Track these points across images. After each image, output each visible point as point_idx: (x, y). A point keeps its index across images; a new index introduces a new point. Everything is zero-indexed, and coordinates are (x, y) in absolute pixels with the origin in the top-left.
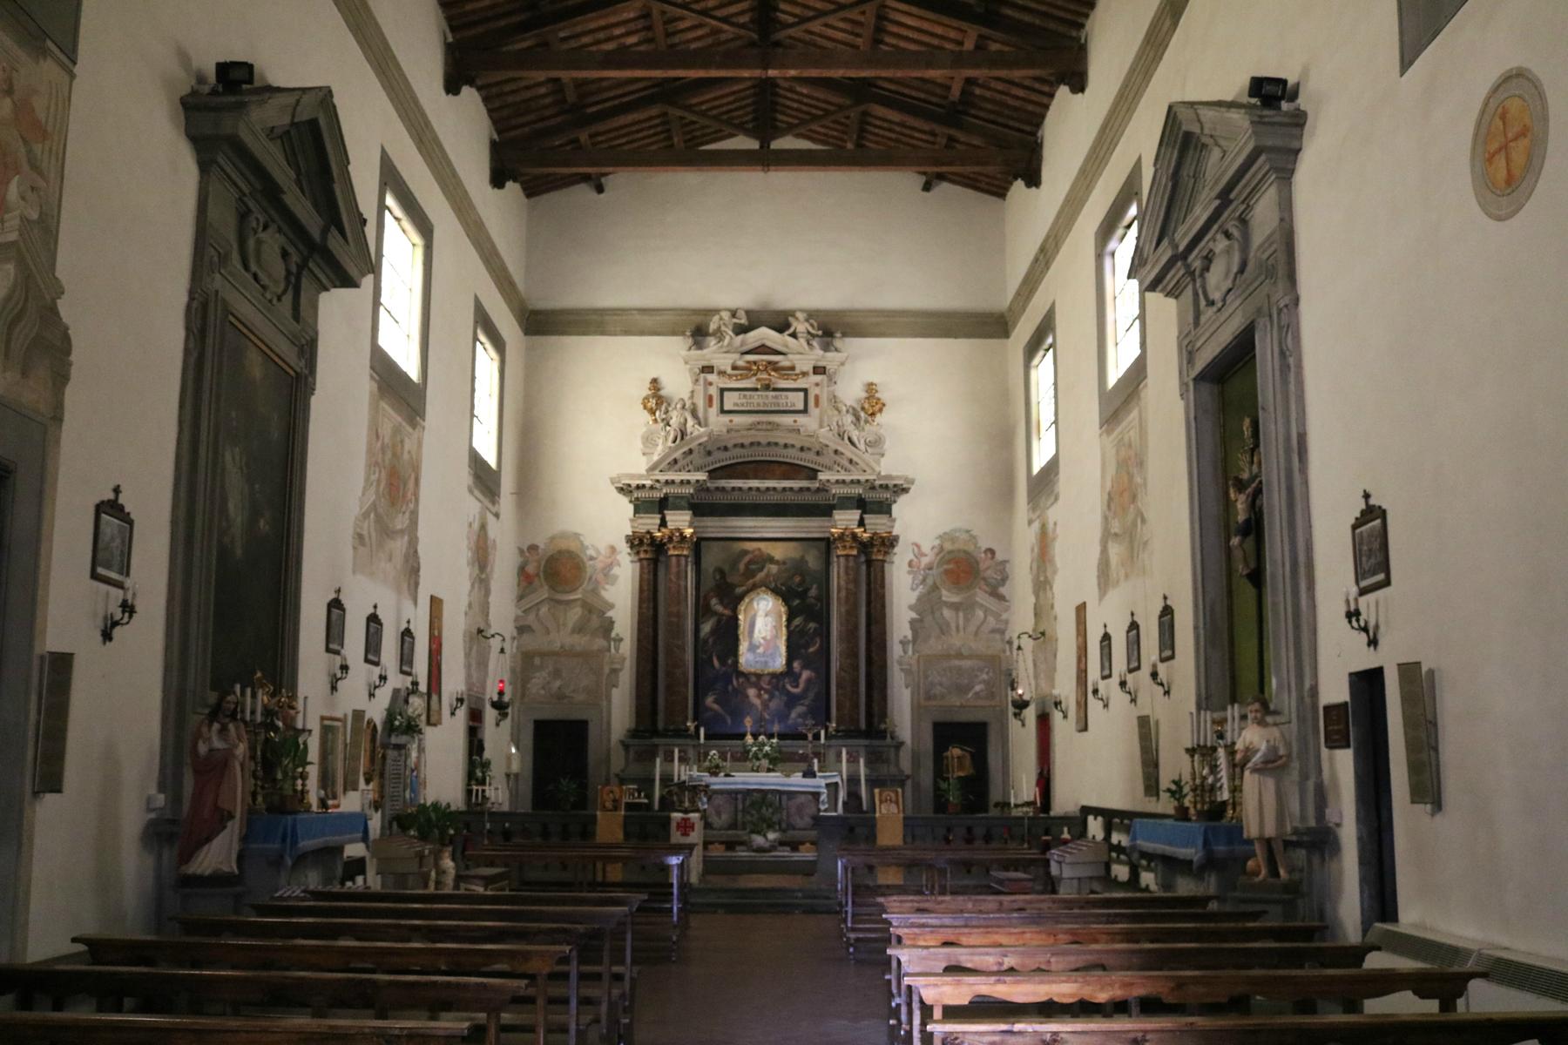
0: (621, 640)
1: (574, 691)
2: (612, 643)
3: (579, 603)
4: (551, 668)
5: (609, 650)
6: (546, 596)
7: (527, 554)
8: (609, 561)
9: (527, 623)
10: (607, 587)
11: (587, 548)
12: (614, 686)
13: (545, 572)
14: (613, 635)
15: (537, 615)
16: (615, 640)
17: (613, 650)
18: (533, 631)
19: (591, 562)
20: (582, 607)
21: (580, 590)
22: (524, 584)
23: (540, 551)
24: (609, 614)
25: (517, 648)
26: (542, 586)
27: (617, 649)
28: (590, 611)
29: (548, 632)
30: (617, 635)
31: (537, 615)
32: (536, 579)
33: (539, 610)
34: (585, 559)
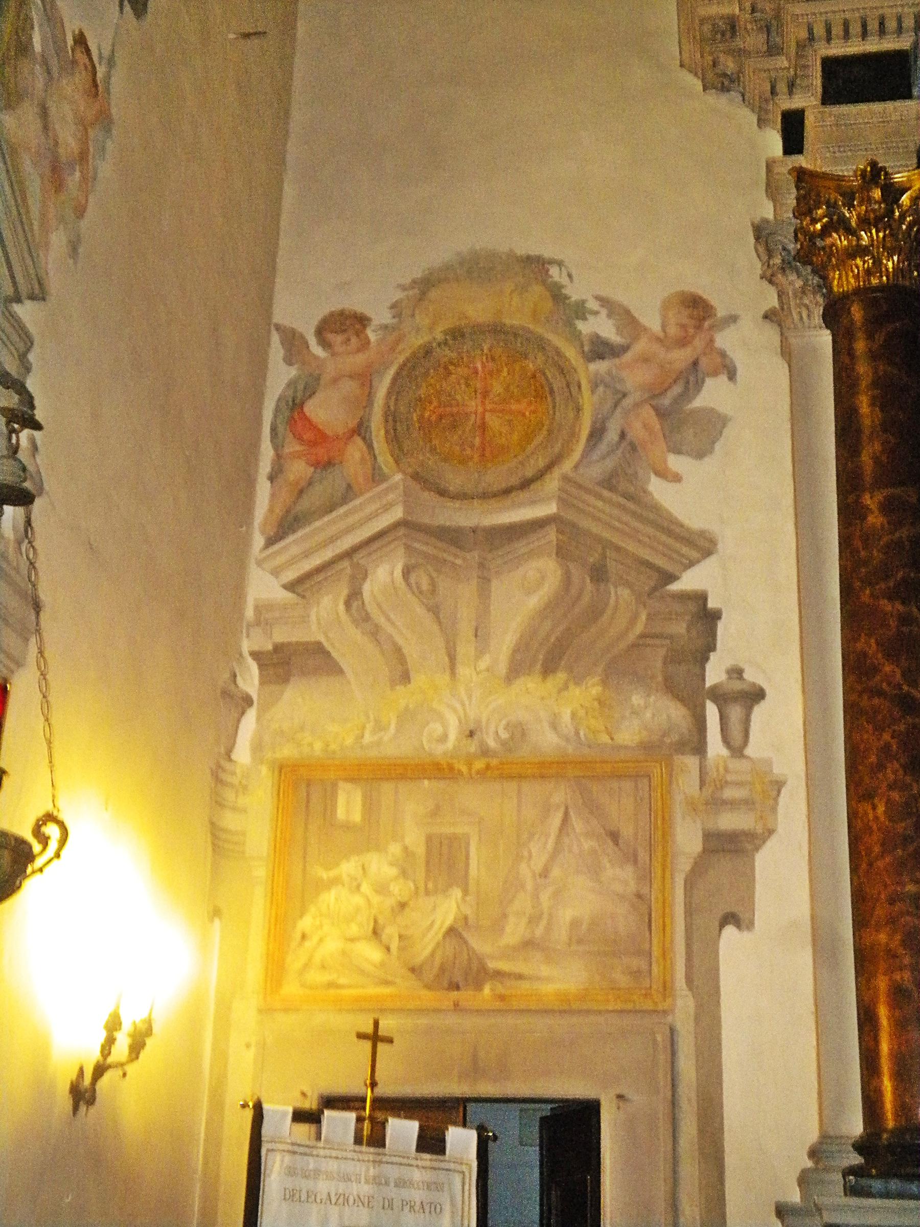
0: (757, 695)
1: (528, 944)
2: (712, 712)
3: (551, 534)
4: (414, 838)
5: (700, 748)
6: (397, 513)
7: (317, 350)
8: (680, 357)
9: (313, 633)
10: (675, 462)
11: (581, 311)
12: (731, 919)
13: (391, 417)
14: (715, 674)
15: (354, 595)
16: (720, 697)
17: (715, 746)
18: (341, 671)
19: (600, 367)
20: (561, 553)
21: (552, 483)
22: (299, 469)
23: (372, 335)
24: (688, 582)
25: (257, 747)
26: (376, 476)
27: (737, 750)
28: (599, 574)
29: (406, 678)
30: (736, 672)
31: (354, 595)
32: (355, 451)
33: (360, 576)
34: (571, 353)
